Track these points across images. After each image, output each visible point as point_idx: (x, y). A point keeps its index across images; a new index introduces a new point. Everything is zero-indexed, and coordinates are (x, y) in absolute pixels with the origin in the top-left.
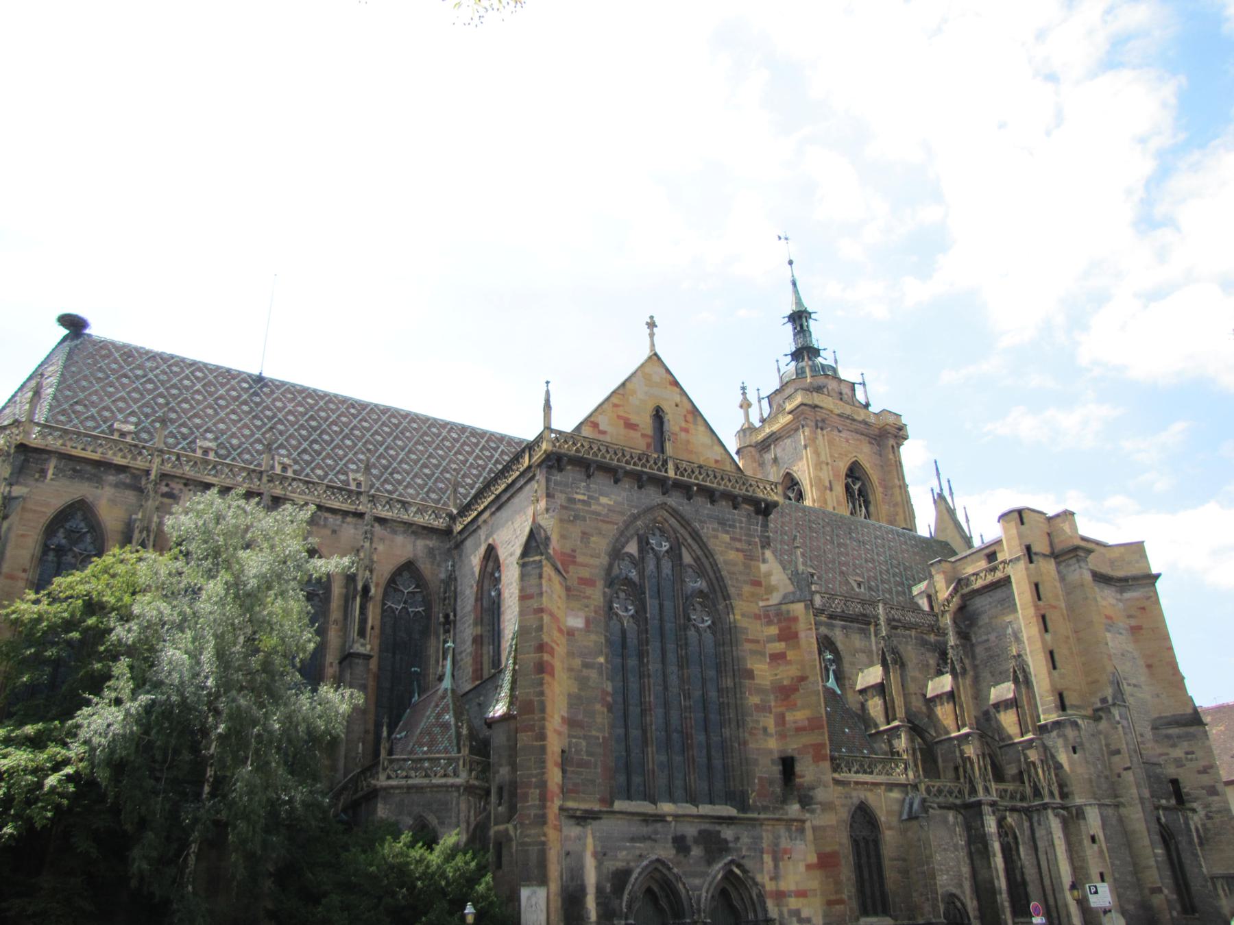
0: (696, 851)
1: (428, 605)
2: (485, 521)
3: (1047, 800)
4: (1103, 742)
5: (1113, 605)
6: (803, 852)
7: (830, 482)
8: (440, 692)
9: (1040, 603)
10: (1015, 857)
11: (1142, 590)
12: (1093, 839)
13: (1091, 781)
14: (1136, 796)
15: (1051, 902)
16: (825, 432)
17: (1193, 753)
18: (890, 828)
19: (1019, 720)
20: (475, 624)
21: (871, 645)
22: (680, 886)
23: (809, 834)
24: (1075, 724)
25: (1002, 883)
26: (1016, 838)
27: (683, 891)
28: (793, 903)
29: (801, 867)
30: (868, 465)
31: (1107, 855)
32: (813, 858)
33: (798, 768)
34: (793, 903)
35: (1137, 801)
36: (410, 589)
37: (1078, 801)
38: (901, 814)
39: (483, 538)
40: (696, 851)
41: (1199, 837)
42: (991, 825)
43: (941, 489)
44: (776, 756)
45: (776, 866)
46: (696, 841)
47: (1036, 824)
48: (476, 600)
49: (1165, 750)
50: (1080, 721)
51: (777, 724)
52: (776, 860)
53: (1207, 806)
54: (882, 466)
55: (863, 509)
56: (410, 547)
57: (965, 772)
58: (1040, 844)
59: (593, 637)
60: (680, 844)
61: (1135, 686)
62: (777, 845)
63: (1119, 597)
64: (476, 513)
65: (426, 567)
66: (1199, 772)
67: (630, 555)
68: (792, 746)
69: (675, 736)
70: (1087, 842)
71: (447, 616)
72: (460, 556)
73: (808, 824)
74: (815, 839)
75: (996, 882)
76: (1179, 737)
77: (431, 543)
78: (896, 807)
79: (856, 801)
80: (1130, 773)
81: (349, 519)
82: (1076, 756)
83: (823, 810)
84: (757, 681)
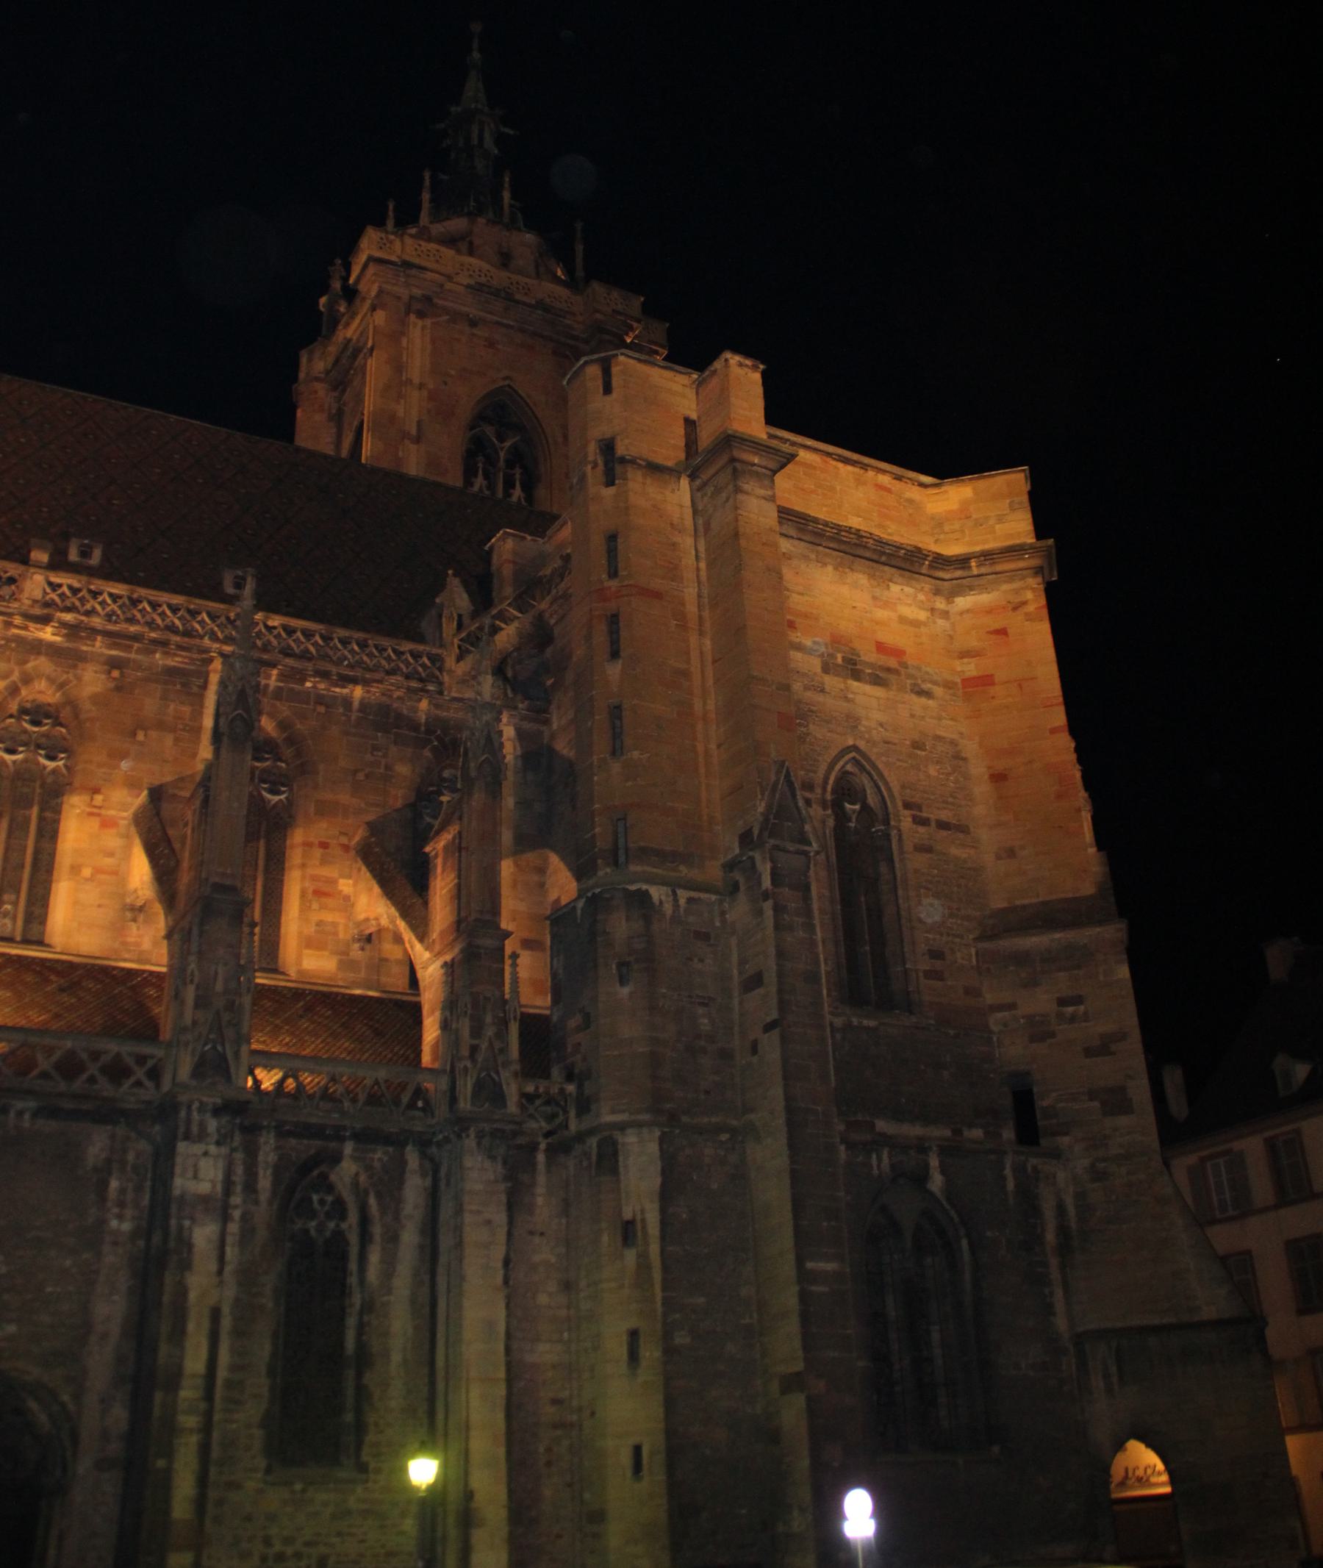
4: (735, 958)
5: (916, 624)
7: (419, 423)
9: (613, 584)
10: (353, 1280)
11: (1005, 587)
14: (780, 1105)
16: (428, 322)
19: (459, 887)
21: (198, 713)
26: (365, 1220)
31: (657, 1276)
35: (780, 1121)
41: (1063, 1230)
47: (442, 1184)
50: (656, 893)
55: (517, 493)
61: (943, 825)
63: (940, 604)
75: (164, 1350)
80: (775, 1033)
82: (625, 991)
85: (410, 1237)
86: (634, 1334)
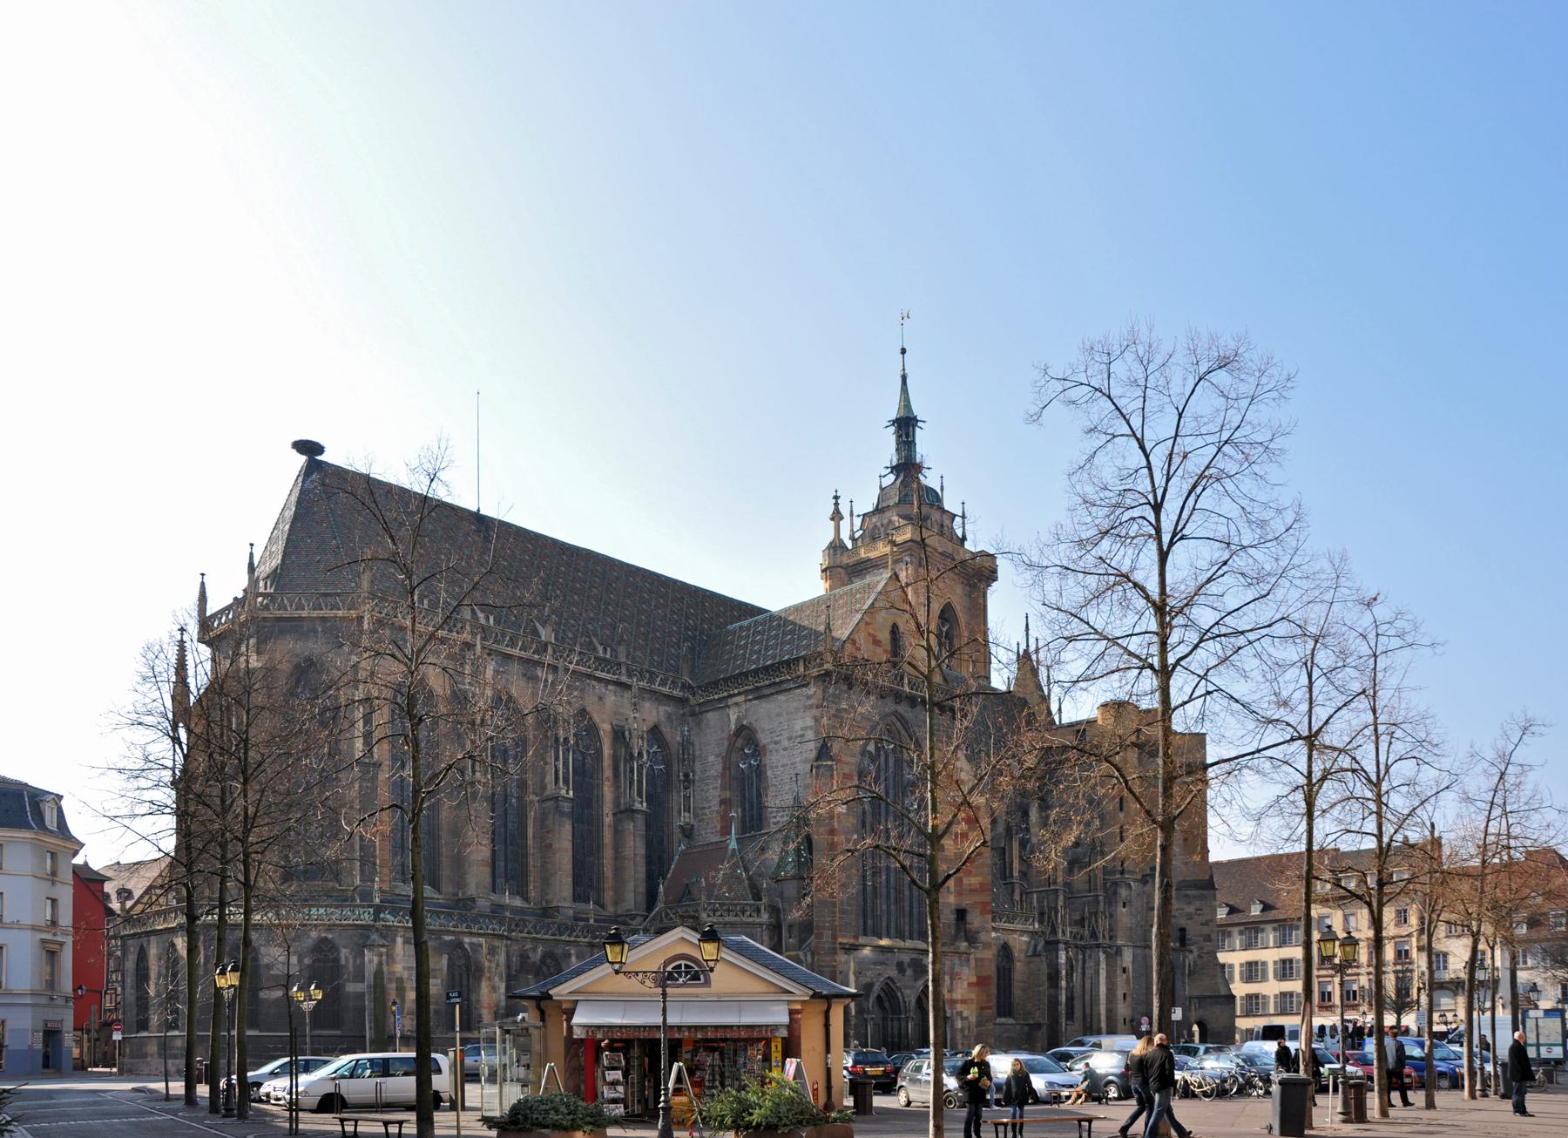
0: (909, 972)
1: (668, 764)
2: (736, 704)
3: (1101, 941)
6: (968, 975)
8: (729, 852)
12: (1124, 970)
13: (1131, 928)
15: (1088, 1011)
17: (1201, 910)
18: (1019, 961)
20: (723, 788)
22: (899, 994)
23: (972, 962)
24: (1129, 885)
25: (1063, 998)
27: (901, 998)
28: (959, 1007)
29: (965, 983)
30: (958, 608)
32: (974, 979)
33: (969, 918)
34: (959, 1007)
36: (654, 749)
37: (1119, 942)
38: (1027, 952)
39: (733, 718)
40: (909, 972)
41: (1189, 970)
42: (1062, 959)
43: (1028, 646)
44: (953, 907)
45: (952, 983)
46: (909, 966)
48: (724, 769)
49: (1182, 906)
51: (955, 886)
52: (952, 979)
53: (1201, 948)
54: (970, 609)
56: (654, 712)
57: (1049, 917)
58: (1088, 972)
59: (851, 819)
60: (901, 967)
62: (953, 969)
64: (726, 694)
65: (666, 730)
66: (1202, 924)
67: (870, 753)
68: (966, 902)
69: (892, 890)
70: (1119, 971)
71: (686, 775)
72: (698, 724)
73: (972, 956)
74: (976, 966)
76: (1194, 897)
77: (669, 709)
78: (1024, 947)
79: (1002, 942)
81: (610, 687)
83: (984, 948)
84: (946, 853)
85: (1080, 970)
86: (1125, 994)
